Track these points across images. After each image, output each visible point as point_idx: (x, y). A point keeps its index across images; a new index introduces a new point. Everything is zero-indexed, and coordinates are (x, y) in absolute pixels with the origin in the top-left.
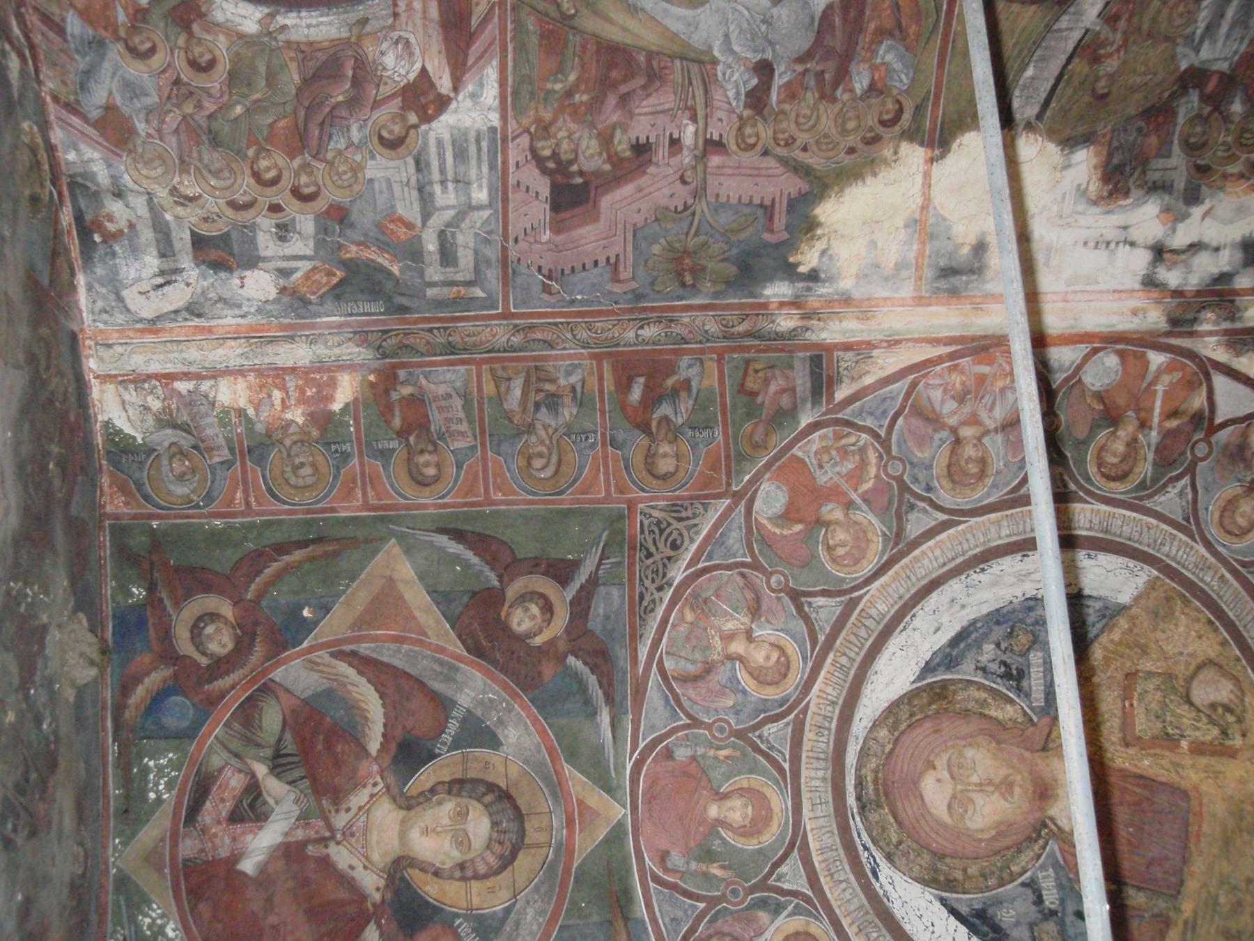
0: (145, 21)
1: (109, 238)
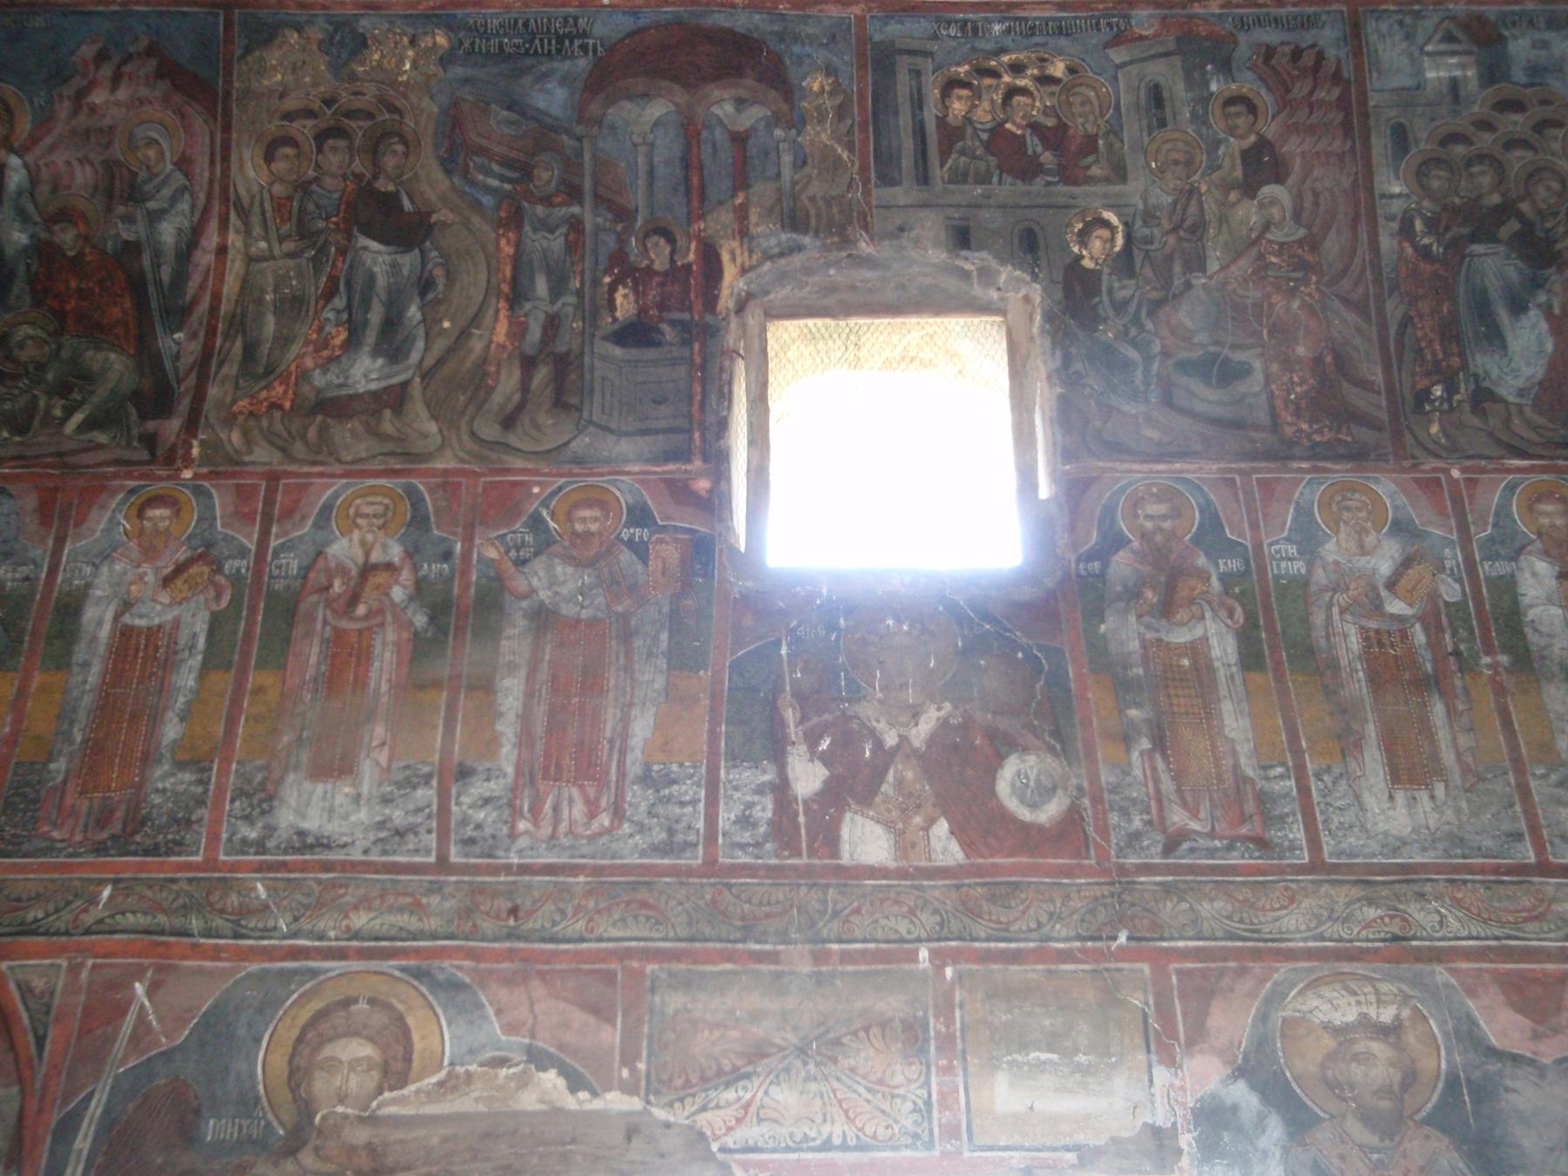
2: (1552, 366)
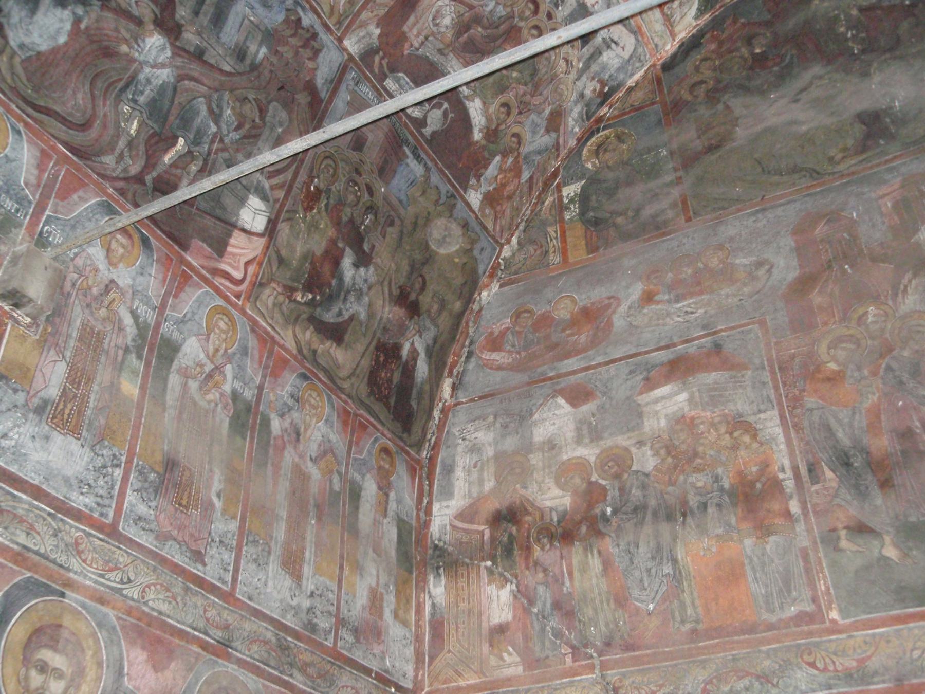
0: (505, 150)
1: (603, 83)
2: (55, 51)
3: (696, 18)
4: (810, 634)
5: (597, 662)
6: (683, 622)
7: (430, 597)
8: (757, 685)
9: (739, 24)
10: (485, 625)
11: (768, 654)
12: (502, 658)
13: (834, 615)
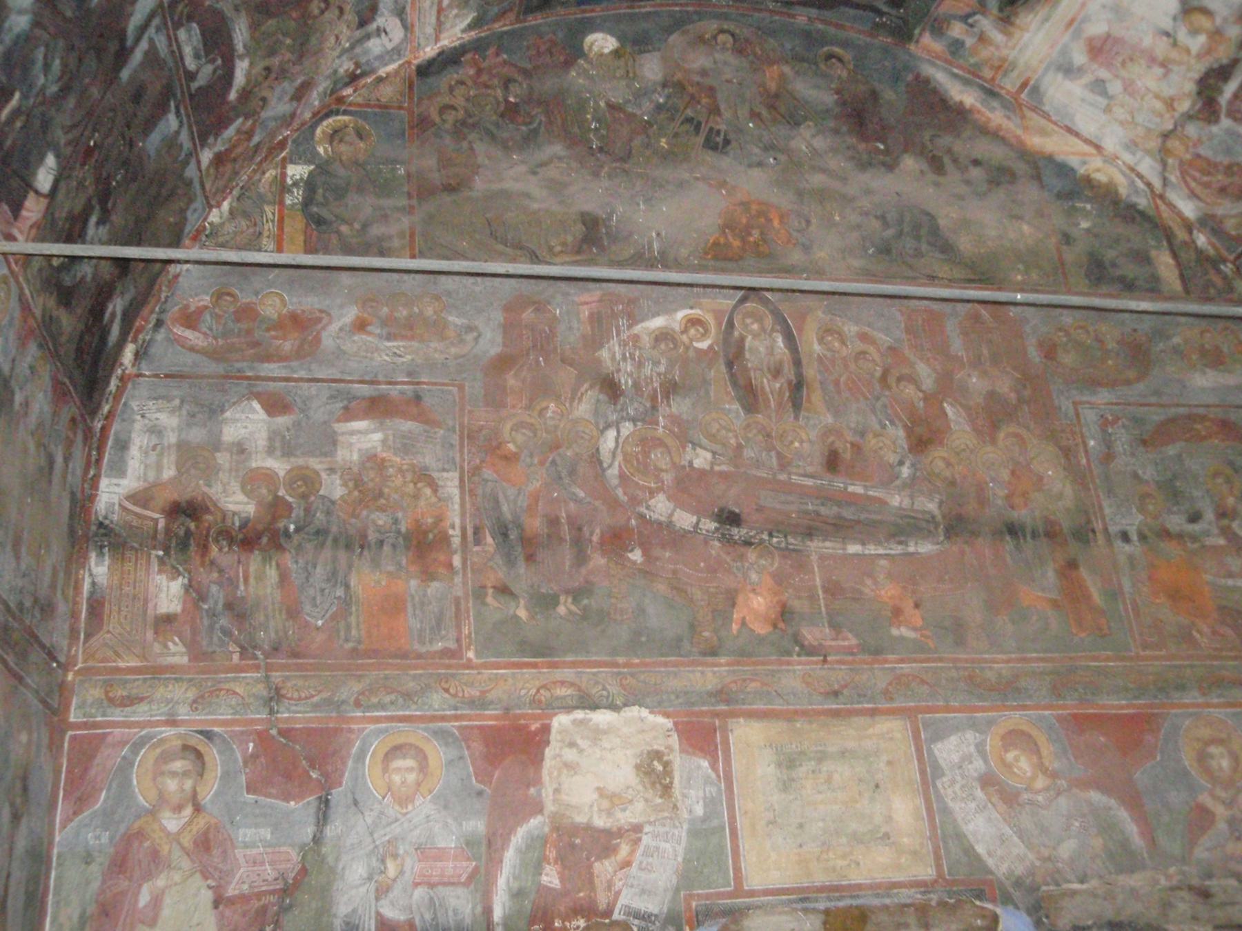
1: (357, 65)
3: (464, 31)
4: (449, 667)
5: (262, 664)
6: (347, 640)
7: (91, 575)
8: (401, 700)
9: (499, 59)
10: (150, 612)
11: (414, 677)
12: (166, 647)
13: (471, 654)
